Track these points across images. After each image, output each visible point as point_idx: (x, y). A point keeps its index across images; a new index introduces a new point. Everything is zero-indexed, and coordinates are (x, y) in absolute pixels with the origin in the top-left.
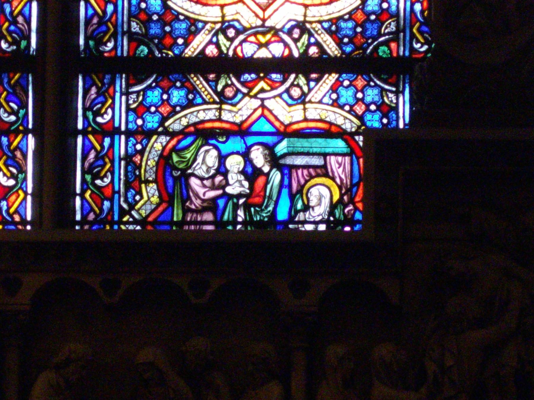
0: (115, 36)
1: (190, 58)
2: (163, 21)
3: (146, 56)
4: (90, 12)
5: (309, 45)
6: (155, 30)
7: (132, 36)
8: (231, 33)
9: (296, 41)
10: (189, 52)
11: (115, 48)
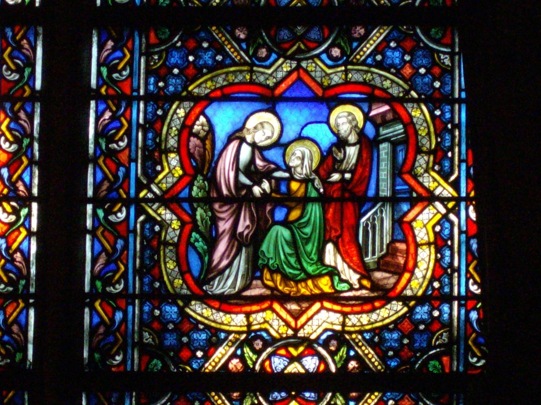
0: (123, 349)
1: (211, 372)
2: (179, 331)
3: (160, 372)
4: (96, 320)
5: (349, 359)
6: (170, 340)
7: (144, 348)
8: (258, 344)
9: (333, 354)
10: (209, 367)
11: (124, 361)
